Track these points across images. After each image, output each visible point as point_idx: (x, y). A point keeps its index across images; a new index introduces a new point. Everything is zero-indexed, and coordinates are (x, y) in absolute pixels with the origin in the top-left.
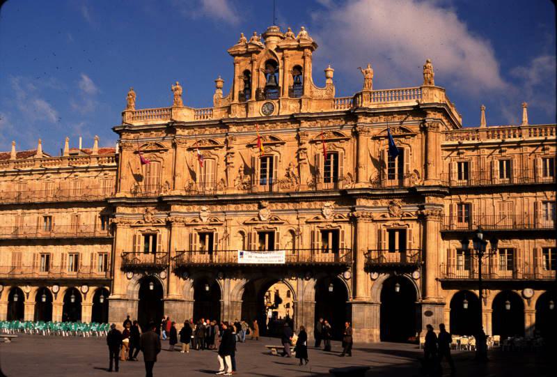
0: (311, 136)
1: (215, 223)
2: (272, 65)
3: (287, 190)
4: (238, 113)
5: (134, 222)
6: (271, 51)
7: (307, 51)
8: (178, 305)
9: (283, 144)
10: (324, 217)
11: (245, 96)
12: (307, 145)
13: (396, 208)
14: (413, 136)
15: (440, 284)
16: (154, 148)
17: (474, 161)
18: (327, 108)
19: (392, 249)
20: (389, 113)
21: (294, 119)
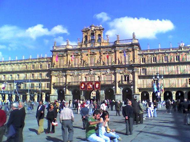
0: (104, 52)
1: (78, 75)
2: (93, 34)
3: (97, 66)
4: (84, 46)
5: (56, 75)
6: (92, 31)
7: (102, 31)
8: (68, 96)
9: (96, 54)
10: (107, 73)
12: (102, 54)
13: (126, 70)
14: (130, 52)
15: (138, 89)
16: (62, 56)
17: (146, 58)
18: (107, 45)
19: (125, 80)
20: (124, 46)
21: (99, 48)
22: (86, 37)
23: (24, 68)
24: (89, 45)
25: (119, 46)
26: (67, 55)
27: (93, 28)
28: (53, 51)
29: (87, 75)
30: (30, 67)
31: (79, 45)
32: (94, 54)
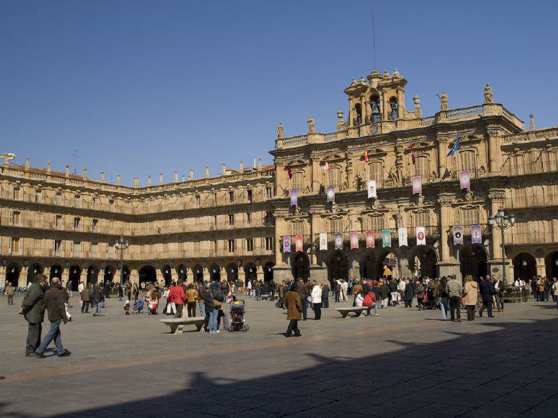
1: (341, 213)
2: (375, 99)
4: (353, 134)
6: (372, 90)
9: (385, 154)
11: (358, 122)
21: (392, 137)
22: (358, 108)
23: (211, 202)
24: (366, 131)
25: (446, 127)
26: (311, 164)
27: (375, 83)
28: (277, 153)
29: (363, 213)
30: (223, 198)
31: (342, 130)
32: (380, 154)
